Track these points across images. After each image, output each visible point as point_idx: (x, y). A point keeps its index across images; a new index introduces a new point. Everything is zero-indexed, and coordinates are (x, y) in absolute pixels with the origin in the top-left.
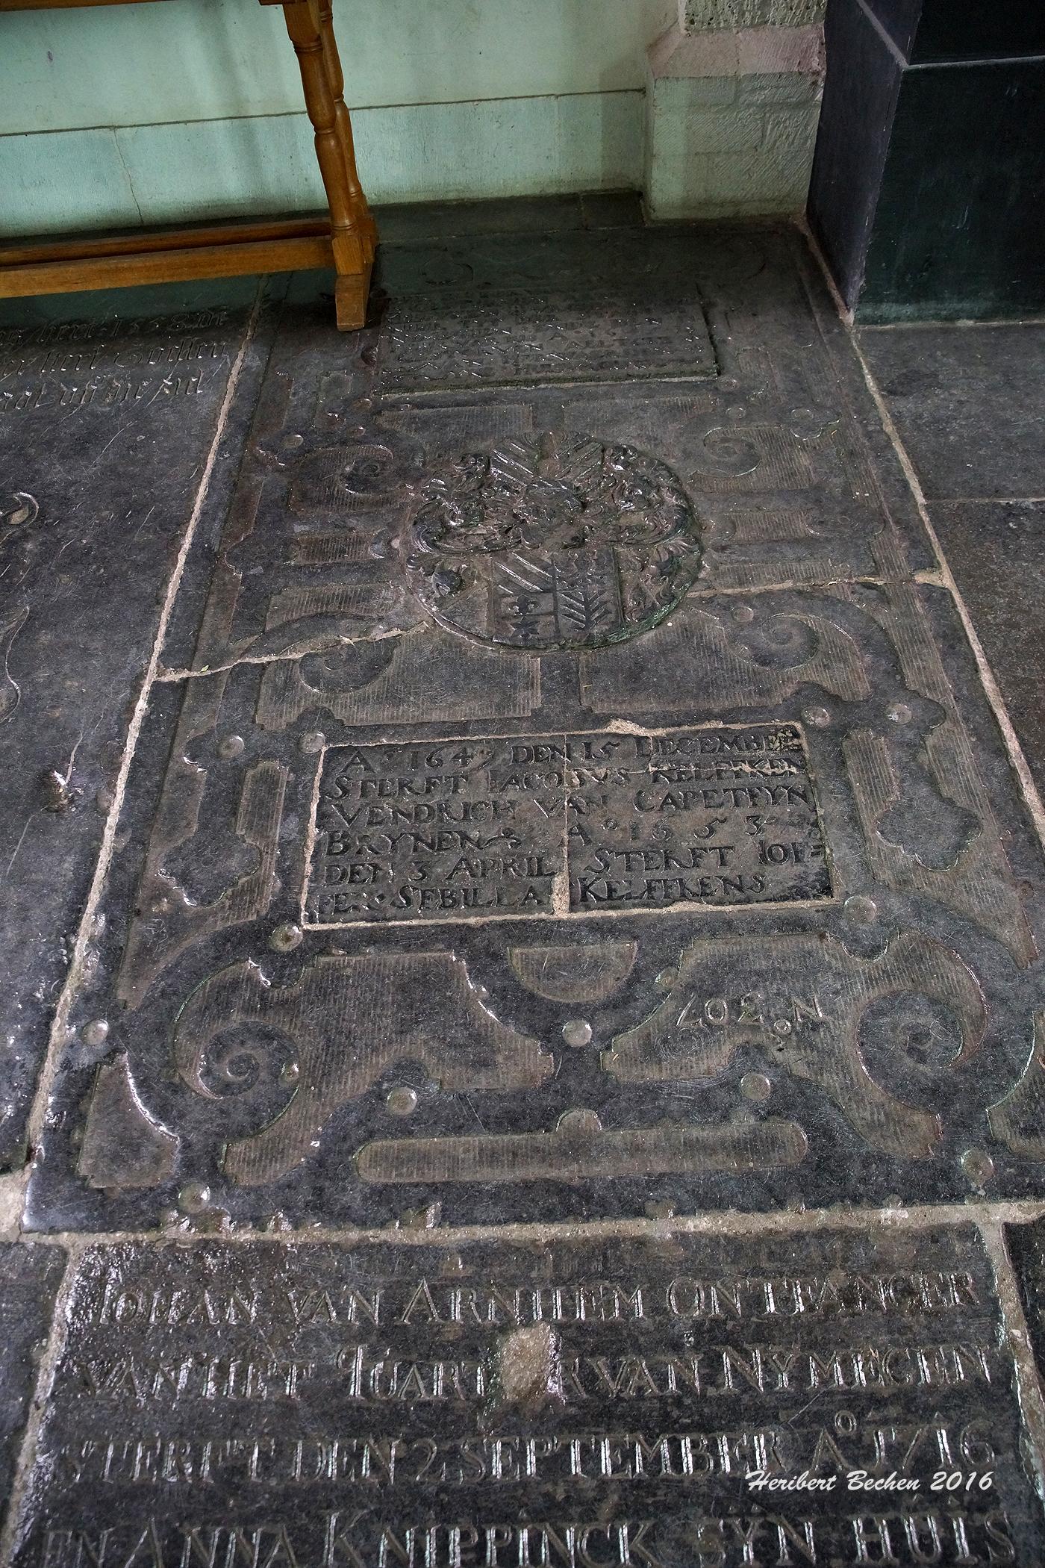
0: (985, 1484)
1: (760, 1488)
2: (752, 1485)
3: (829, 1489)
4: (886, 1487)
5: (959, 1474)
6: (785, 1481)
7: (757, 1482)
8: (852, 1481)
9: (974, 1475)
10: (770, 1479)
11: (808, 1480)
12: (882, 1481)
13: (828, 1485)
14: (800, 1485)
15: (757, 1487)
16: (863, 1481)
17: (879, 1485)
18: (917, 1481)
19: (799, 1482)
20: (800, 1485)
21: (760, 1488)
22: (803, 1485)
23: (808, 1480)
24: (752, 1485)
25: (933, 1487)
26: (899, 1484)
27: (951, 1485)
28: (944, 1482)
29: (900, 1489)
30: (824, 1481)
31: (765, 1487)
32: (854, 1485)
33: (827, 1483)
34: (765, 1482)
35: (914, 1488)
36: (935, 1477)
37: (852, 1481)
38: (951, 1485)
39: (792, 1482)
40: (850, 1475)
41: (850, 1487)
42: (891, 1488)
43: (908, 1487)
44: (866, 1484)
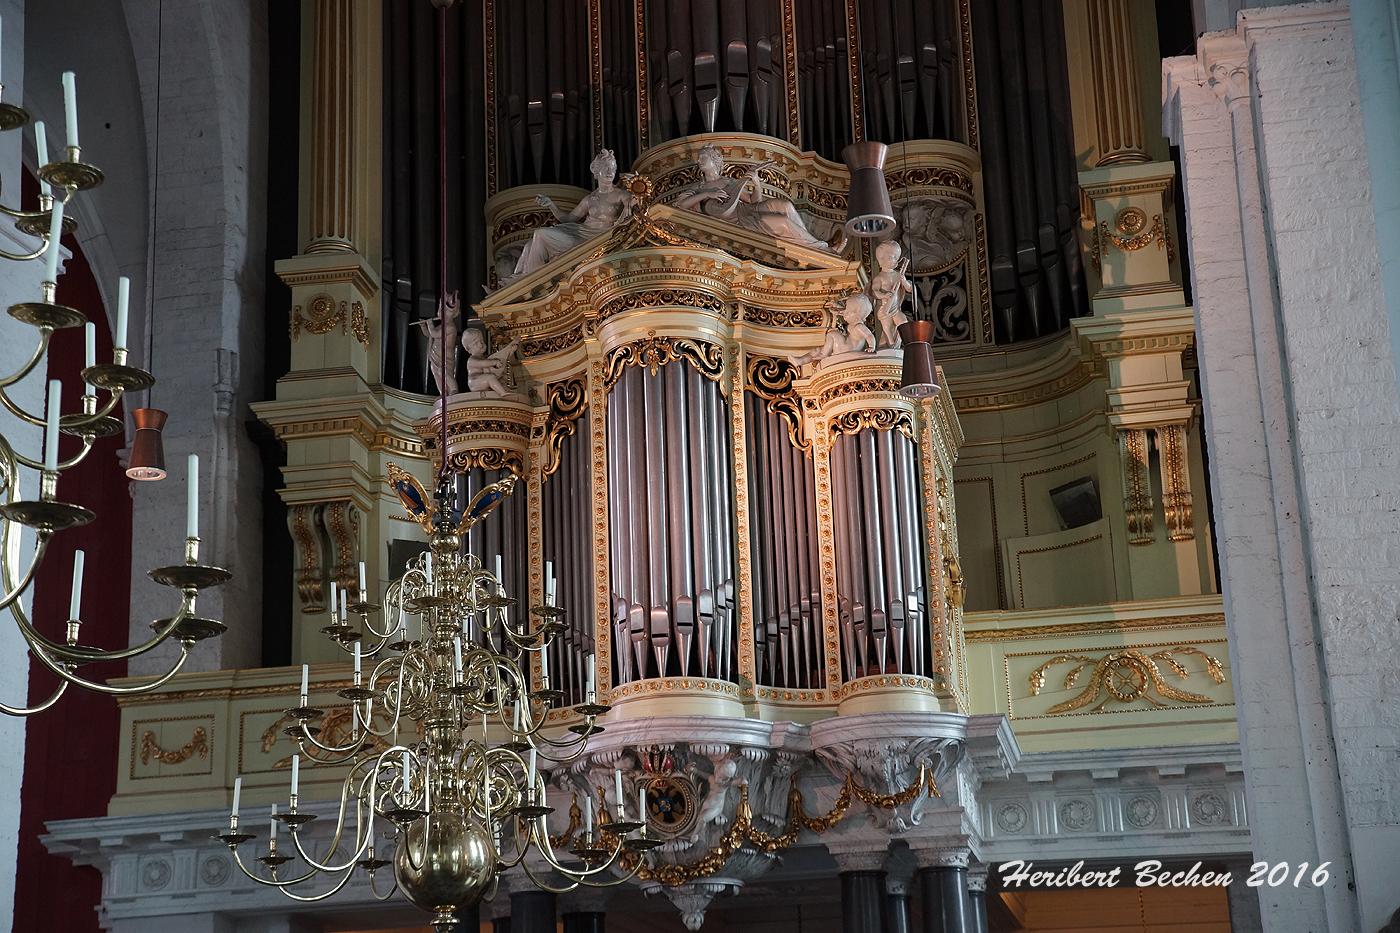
0: (1319, 878)
1: (1018, 884)
2: (1007, 880)
3: (1110, 885)
4: (1186, 882)
5: (1284, 864)
6: (1052, 875)
7: (1015, 876)
8: (1141, 875)
9: (1305, 866)
10: (1031, 872)
11: (1082, 873)
12: (1181, 875)
13: (1110, 880)
14: (1072, 880)
15: (1014, 882)
16: (1157, 874)
17: (1178, 881)
18: (1229, 875)
19: (1070, 876)
20: (1072, 880)
21: (1018, 884)
22: (1076, 880)
23: (1082, 873)
24: (1007, 880)
25: (1250, 883)
26: (1205, 878)
27: (1274, 881)
28: (1265, 876)
29: (1206, 885)
30: (1104, 875)
31: (1025, 883)
32: (1145, 879)
33: (1108, 877)
34: (1025, 876)
35: (1225, 884)
36: (1252, 870)
37: (1141, 875)
38: (1274, 881)
39: (1061, 876)
40: (1139, 866)
41: (1139, 883)
42: (1194, 884)
43: (1217, 882)
44: (1161, 878)
